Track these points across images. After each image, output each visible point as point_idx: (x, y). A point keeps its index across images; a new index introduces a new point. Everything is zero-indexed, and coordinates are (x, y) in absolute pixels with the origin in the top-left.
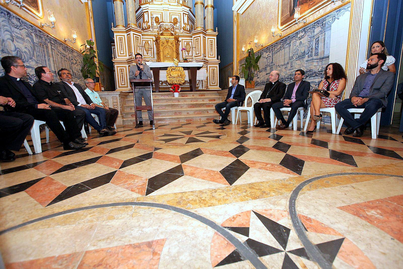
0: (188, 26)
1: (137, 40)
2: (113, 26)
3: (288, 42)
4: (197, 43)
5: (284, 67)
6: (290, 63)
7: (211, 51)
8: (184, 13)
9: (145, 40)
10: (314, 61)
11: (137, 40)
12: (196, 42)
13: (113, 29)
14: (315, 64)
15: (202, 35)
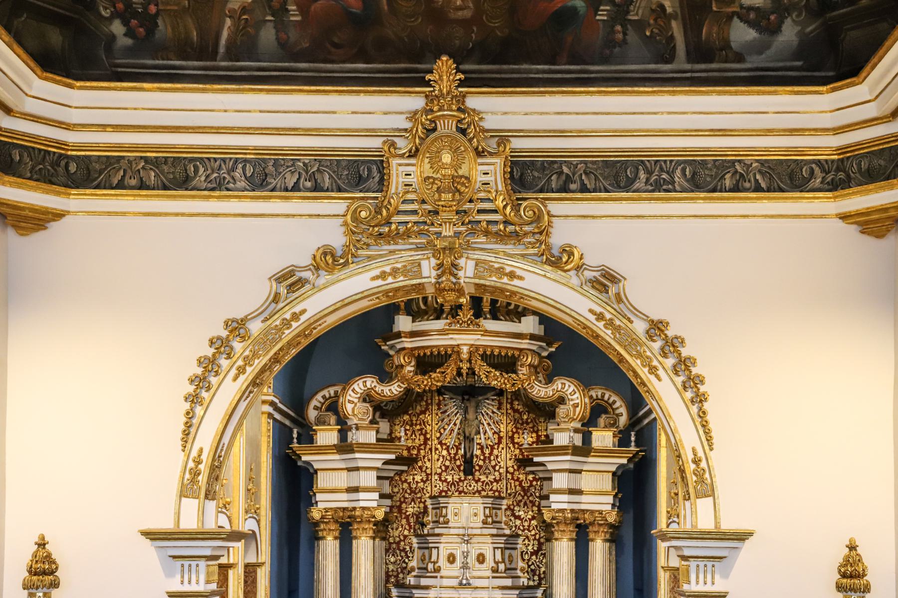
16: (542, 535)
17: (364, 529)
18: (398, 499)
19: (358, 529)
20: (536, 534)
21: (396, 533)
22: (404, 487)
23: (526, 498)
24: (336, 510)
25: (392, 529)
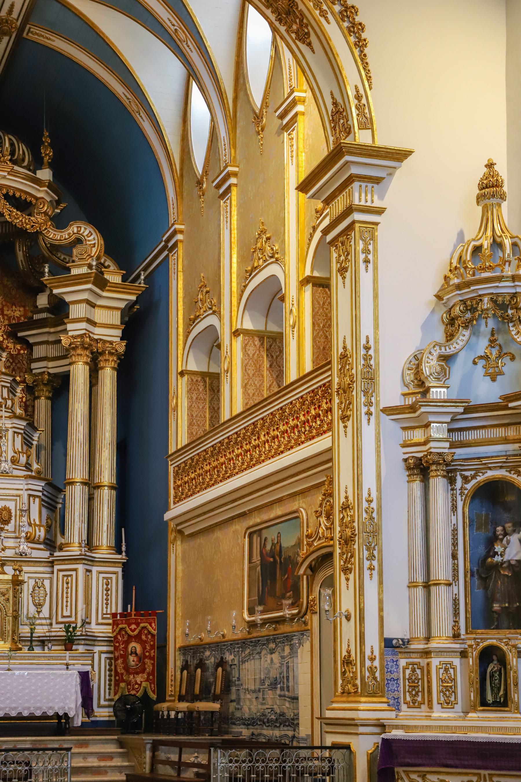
0: (42, 529)
3: (258, 649)
4: (67, 588)
5: (255, 695)
6: (261, 690)
7: (107, 608)
8: (30, 496)
10: (286, 698)
12: (65, 585)
14: (287, 705)
15: (81, 568)
16: (28, 398)
20: (23, 397)
23: (14, 364)
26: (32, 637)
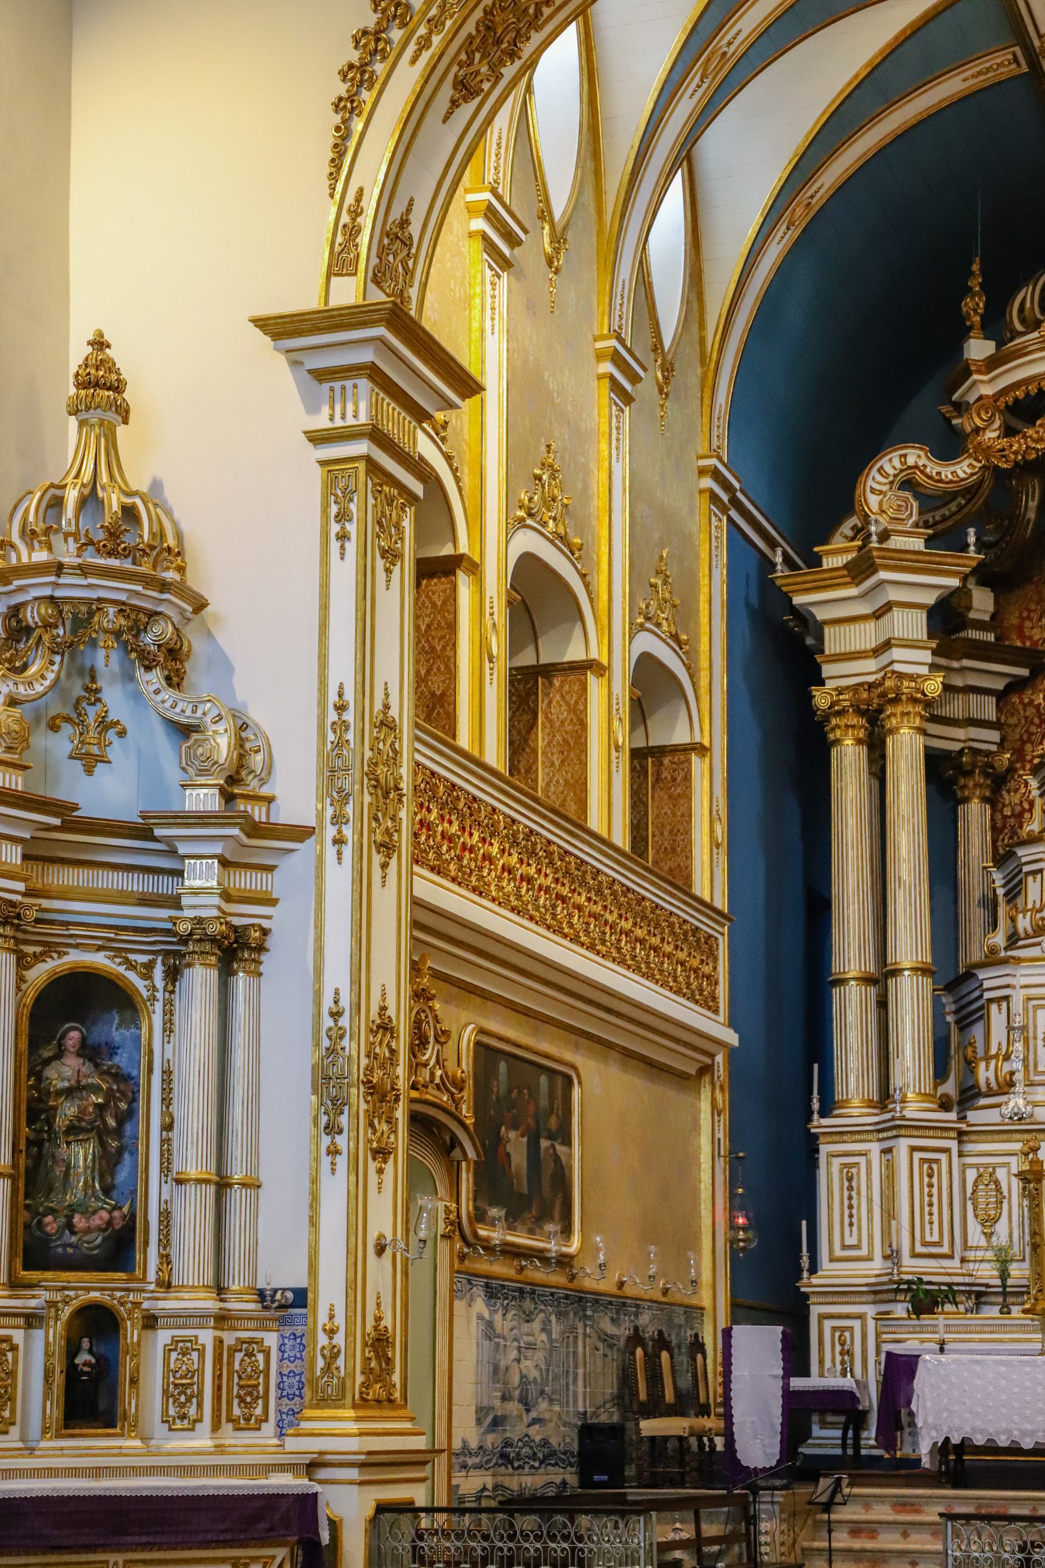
1: (930, 1176)
2: (816, 1105)
9: (977, 1166)
11: (930, 1176)
13: (819, 1124)
17: (904, 714)
18: (1018, 737)
19: (894, 715)
21: (1016, 798)
22: (1028, 714)
24: (855, 688)
25: (1008, 791)
26: (1004, 1286)
